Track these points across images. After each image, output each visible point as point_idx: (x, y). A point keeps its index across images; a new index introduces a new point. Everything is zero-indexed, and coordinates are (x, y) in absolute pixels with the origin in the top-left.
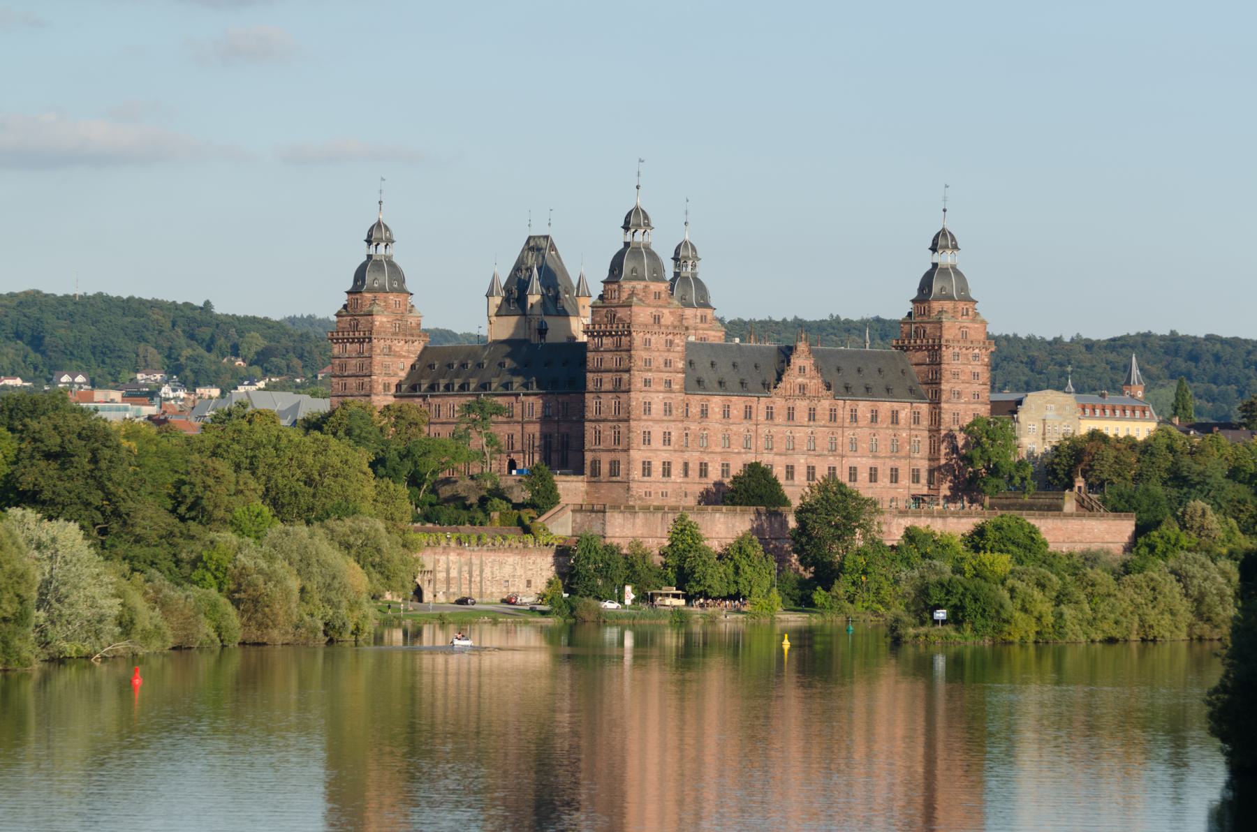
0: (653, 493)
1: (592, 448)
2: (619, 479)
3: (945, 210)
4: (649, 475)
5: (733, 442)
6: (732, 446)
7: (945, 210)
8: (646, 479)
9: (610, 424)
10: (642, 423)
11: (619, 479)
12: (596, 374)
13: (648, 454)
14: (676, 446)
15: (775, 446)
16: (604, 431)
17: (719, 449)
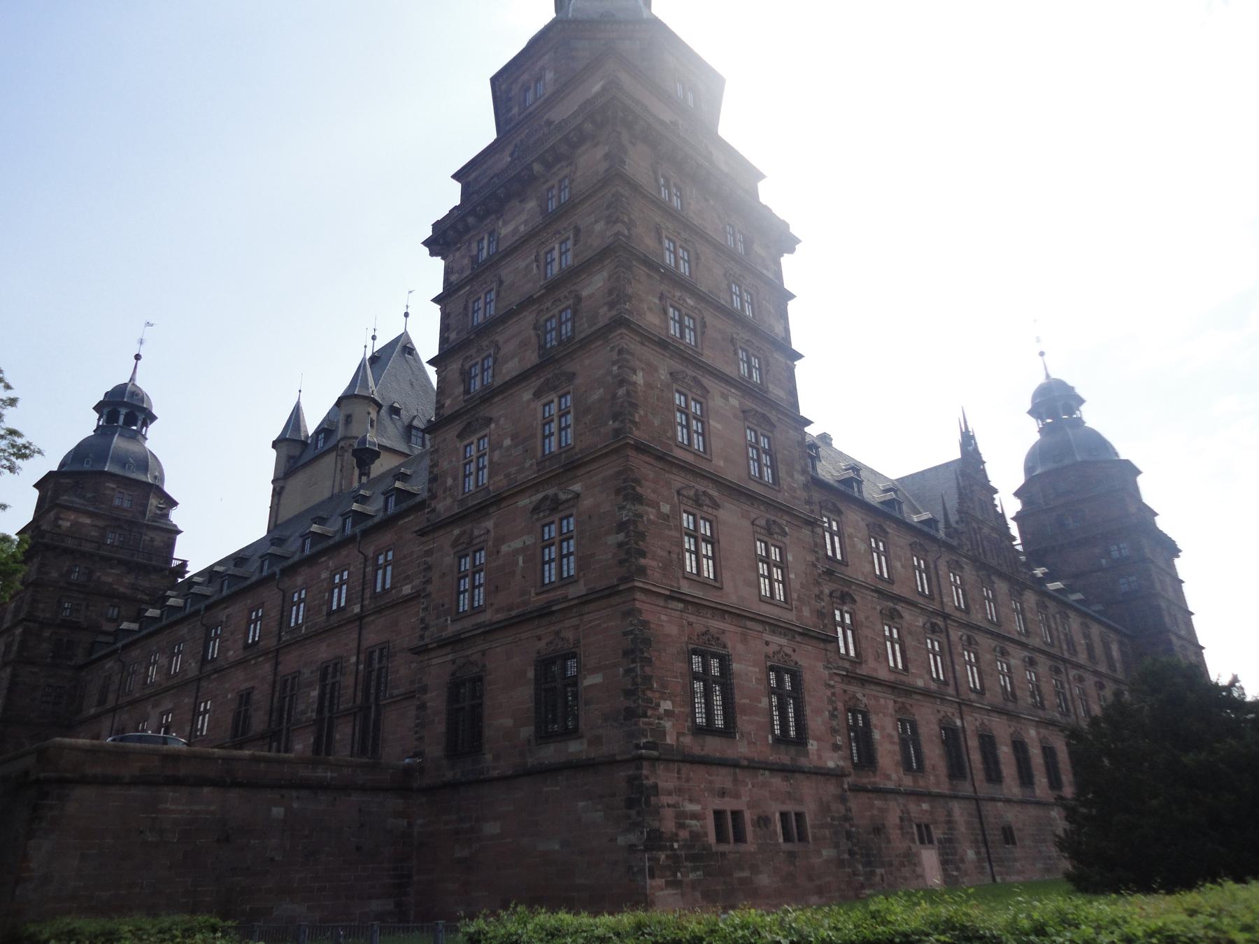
0: (748, 816)
1: (452, 629)
2: (575, 748)
3: (1042, 354)
4: (729, 731)
5: (910, 654)
6: (913, 670)
7: (1042, 354)
8: (712, 746)
9: (525, 502)
10: (678, 480)
11: (575, 748)
12: (473, 351)
13: (715, 624)
14: (806, 612)
15: (987, 683)
16: (500, 540)
17: (883, 674)
